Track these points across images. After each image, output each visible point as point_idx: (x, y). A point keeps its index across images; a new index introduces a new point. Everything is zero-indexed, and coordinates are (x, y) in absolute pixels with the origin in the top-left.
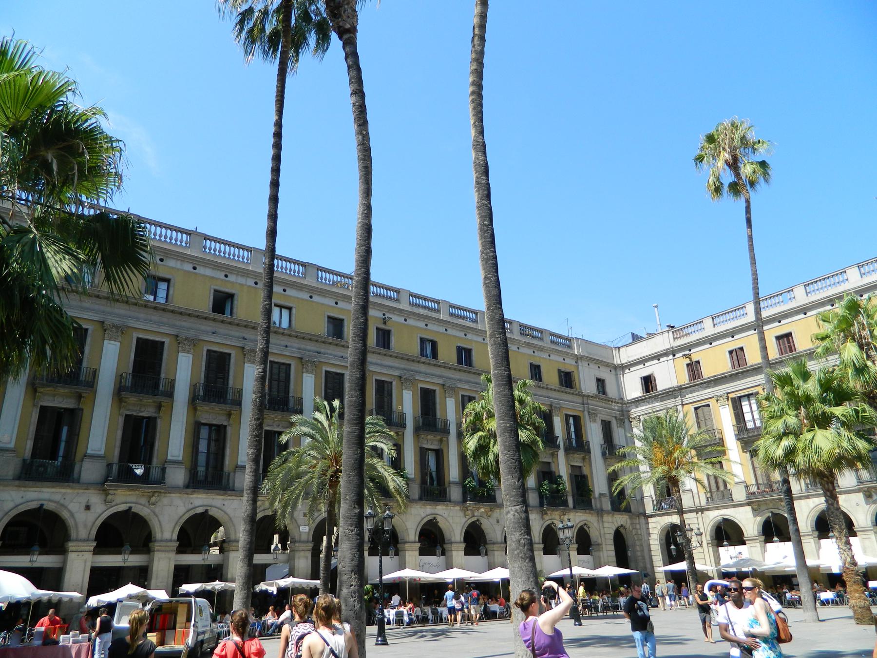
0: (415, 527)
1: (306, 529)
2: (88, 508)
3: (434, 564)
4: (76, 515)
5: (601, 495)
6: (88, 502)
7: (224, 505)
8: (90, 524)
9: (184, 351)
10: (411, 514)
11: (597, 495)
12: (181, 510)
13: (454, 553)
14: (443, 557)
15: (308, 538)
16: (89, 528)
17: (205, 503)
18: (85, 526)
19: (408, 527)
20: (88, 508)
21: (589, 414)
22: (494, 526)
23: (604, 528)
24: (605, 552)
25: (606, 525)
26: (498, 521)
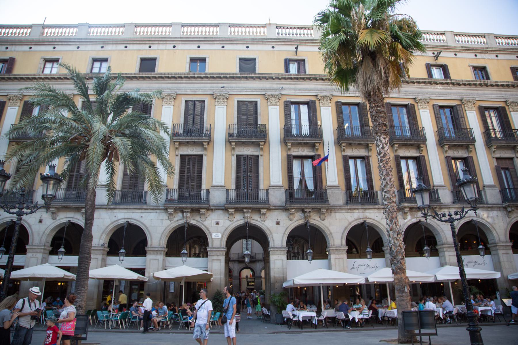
0: (342, 232)
1: (219, 235)
3: (370, 266)
4: (33, 227)
6: (41, 218)
7: (142, 217)
8: (41, 233)
10: (336, 219)
12: (108, 222)
15: (221, 245)
16: (40, 236)
17: (126, 217)
18: (39, 235)
19: (332, 231)
20: (41, 221)
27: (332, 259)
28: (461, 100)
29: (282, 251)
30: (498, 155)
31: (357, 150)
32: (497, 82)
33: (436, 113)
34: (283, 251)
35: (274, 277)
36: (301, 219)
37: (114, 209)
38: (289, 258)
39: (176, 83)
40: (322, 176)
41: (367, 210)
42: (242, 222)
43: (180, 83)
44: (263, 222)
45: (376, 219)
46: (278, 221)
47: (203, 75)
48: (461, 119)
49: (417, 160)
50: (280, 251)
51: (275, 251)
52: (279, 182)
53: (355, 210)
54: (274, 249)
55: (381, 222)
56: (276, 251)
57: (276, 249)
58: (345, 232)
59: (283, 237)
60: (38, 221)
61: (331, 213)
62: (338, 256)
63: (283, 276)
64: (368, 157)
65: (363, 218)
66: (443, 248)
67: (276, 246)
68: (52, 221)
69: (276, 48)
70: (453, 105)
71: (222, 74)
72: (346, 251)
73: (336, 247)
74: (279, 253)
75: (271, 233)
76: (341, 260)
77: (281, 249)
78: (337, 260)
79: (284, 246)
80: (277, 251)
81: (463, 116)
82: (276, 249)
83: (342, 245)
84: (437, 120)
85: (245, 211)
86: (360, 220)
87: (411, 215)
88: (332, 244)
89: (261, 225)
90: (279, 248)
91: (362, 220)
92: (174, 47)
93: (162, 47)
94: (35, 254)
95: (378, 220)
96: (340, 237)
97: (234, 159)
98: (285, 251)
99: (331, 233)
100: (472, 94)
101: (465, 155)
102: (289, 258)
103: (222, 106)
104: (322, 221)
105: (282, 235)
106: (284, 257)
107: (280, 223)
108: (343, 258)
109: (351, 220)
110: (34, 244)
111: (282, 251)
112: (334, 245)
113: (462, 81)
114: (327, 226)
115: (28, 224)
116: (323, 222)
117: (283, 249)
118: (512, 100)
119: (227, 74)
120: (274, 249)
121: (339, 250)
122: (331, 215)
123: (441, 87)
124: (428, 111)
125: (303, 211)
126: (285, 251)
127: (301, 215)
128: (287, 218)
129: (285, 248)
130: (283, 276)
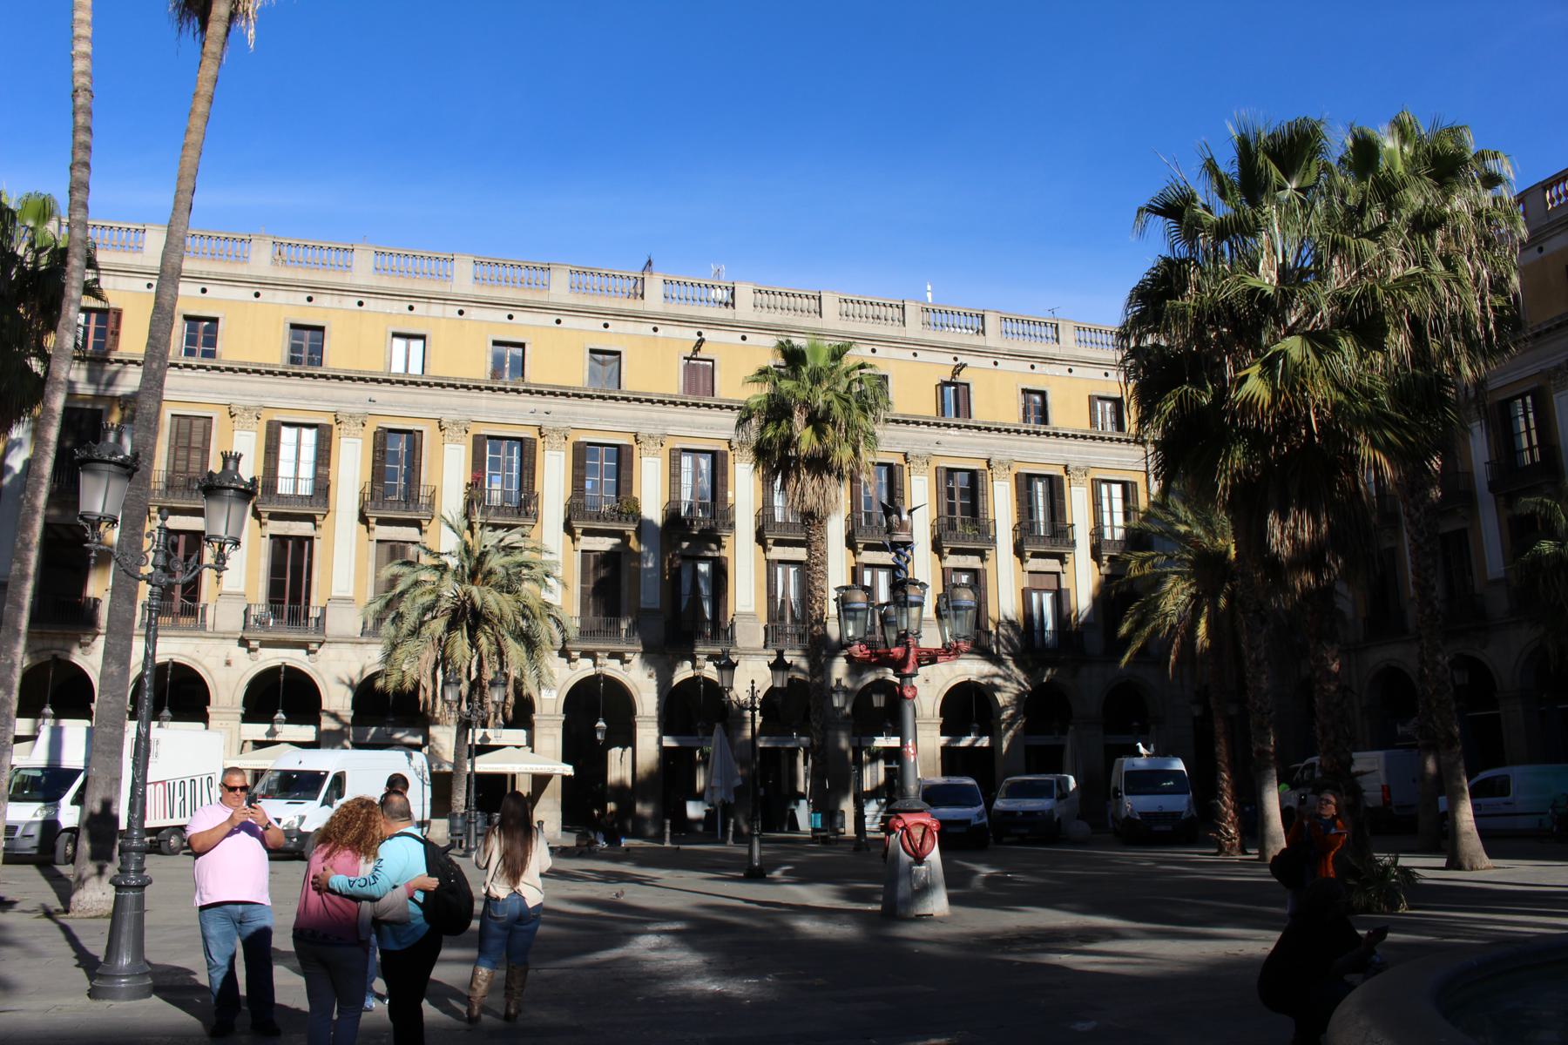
1: (554, 694)
2: (228, 663)
9: (348, 435)
32: (1057, 428)
37: (367, 643)
39: (468, 397)
42: (591, 672)
43: (477, 398)
47: (521, 388)
49: (893, 569)
60: (224, 663)
68: (251, 664)
69: (661, 332)
71: (558, 387)
75: (639, 693)
85: (599, 654)
92: (461, 313)
93: (436, 309)
94: (224, 722)
97: (578, 556)
100: (1010, 448)
103: (558, 453)
110: (220, 705)
113: (995, 423)
115: (205, 668)
119: (569, 388)
123: (956, 433)
124: (926, 478)
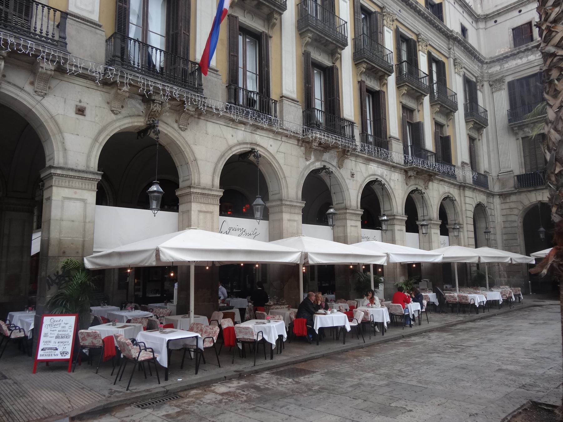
0: (215, 160)
3: (247, 231)
5: (463, 163)
10: (207, 134)
11: (459, 164)
13: (286, 216)
14: (264, 223)
19: (198, 156)
21: (455, 65)
22: (347, 181)
23: (465, 203)
24: (466, 233)
25: (468, 200)
26: (352, 175)
27: (193, 212)
28: (381, 8)
29: (86, 179)
30: (404, 102)
31: (251, 16)
33: (356, 10)
34: (90, 179)
35: (60, 242)
36: (139, 116)
38: (101, 200)
40: (189, 36)
41: (259, 130)
44: (39, 98)
45: (270, 149)
46: (82, 104)
48: (379, 34)
50: (82, 178)
51: (67, 176)
52: (92, 12)
53: (240, 125)
54: (64, 173)
55: (276, 157)
56: (71, 177)
57: (71, 173)
58: (221, 162)
59: (92, 147)
61: (199, 118)
62: (204, 207)
63: (84, 241)
64: (268, 37)
65: (251, 144)
66: (346, 213)
67: (71, 164)
70: (373, 10)
72: (219, 198)
73: (204, 189)
74: (77, 183)
75: (60, 132)
76: (209, 215)
77: (85, 175)
78: (202, 216)
79: (92, 170)
80: (74, 177)
81: (381, 31)
82: (71, 173)
83: (213, 185)
84: (356, 22)
86: (245, 146)
87: (315, 156)
88: (196, 181)
89: (33, 103)
90: (79, 171)
91: (249, 146)
95: (272, 152)
96: (211, 170)
98: (93, 180)
99: (195, 160)
101: (377, 88)
102: (101, 200)
104: (181, 131)
105: (89, 141)
106: (91, 196)
107: (87, 112)
108: (211, 213)
109: (232, 141)
111: (86, 179)
112: (199, 183)
114: (189, 142)
116: (182, 133)
117: (91, 176)
118: (423, 37)
120: (64, 173)
121: (208, 195)
122: (197, 123)
125: (147, 100)
126: (93, 180)
127: (138, 105)
128: (106, 106)
129: (94, 173)
130: (84, 241)
